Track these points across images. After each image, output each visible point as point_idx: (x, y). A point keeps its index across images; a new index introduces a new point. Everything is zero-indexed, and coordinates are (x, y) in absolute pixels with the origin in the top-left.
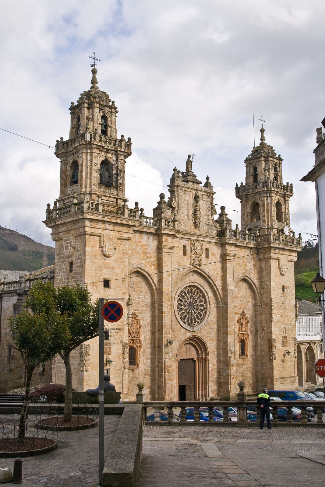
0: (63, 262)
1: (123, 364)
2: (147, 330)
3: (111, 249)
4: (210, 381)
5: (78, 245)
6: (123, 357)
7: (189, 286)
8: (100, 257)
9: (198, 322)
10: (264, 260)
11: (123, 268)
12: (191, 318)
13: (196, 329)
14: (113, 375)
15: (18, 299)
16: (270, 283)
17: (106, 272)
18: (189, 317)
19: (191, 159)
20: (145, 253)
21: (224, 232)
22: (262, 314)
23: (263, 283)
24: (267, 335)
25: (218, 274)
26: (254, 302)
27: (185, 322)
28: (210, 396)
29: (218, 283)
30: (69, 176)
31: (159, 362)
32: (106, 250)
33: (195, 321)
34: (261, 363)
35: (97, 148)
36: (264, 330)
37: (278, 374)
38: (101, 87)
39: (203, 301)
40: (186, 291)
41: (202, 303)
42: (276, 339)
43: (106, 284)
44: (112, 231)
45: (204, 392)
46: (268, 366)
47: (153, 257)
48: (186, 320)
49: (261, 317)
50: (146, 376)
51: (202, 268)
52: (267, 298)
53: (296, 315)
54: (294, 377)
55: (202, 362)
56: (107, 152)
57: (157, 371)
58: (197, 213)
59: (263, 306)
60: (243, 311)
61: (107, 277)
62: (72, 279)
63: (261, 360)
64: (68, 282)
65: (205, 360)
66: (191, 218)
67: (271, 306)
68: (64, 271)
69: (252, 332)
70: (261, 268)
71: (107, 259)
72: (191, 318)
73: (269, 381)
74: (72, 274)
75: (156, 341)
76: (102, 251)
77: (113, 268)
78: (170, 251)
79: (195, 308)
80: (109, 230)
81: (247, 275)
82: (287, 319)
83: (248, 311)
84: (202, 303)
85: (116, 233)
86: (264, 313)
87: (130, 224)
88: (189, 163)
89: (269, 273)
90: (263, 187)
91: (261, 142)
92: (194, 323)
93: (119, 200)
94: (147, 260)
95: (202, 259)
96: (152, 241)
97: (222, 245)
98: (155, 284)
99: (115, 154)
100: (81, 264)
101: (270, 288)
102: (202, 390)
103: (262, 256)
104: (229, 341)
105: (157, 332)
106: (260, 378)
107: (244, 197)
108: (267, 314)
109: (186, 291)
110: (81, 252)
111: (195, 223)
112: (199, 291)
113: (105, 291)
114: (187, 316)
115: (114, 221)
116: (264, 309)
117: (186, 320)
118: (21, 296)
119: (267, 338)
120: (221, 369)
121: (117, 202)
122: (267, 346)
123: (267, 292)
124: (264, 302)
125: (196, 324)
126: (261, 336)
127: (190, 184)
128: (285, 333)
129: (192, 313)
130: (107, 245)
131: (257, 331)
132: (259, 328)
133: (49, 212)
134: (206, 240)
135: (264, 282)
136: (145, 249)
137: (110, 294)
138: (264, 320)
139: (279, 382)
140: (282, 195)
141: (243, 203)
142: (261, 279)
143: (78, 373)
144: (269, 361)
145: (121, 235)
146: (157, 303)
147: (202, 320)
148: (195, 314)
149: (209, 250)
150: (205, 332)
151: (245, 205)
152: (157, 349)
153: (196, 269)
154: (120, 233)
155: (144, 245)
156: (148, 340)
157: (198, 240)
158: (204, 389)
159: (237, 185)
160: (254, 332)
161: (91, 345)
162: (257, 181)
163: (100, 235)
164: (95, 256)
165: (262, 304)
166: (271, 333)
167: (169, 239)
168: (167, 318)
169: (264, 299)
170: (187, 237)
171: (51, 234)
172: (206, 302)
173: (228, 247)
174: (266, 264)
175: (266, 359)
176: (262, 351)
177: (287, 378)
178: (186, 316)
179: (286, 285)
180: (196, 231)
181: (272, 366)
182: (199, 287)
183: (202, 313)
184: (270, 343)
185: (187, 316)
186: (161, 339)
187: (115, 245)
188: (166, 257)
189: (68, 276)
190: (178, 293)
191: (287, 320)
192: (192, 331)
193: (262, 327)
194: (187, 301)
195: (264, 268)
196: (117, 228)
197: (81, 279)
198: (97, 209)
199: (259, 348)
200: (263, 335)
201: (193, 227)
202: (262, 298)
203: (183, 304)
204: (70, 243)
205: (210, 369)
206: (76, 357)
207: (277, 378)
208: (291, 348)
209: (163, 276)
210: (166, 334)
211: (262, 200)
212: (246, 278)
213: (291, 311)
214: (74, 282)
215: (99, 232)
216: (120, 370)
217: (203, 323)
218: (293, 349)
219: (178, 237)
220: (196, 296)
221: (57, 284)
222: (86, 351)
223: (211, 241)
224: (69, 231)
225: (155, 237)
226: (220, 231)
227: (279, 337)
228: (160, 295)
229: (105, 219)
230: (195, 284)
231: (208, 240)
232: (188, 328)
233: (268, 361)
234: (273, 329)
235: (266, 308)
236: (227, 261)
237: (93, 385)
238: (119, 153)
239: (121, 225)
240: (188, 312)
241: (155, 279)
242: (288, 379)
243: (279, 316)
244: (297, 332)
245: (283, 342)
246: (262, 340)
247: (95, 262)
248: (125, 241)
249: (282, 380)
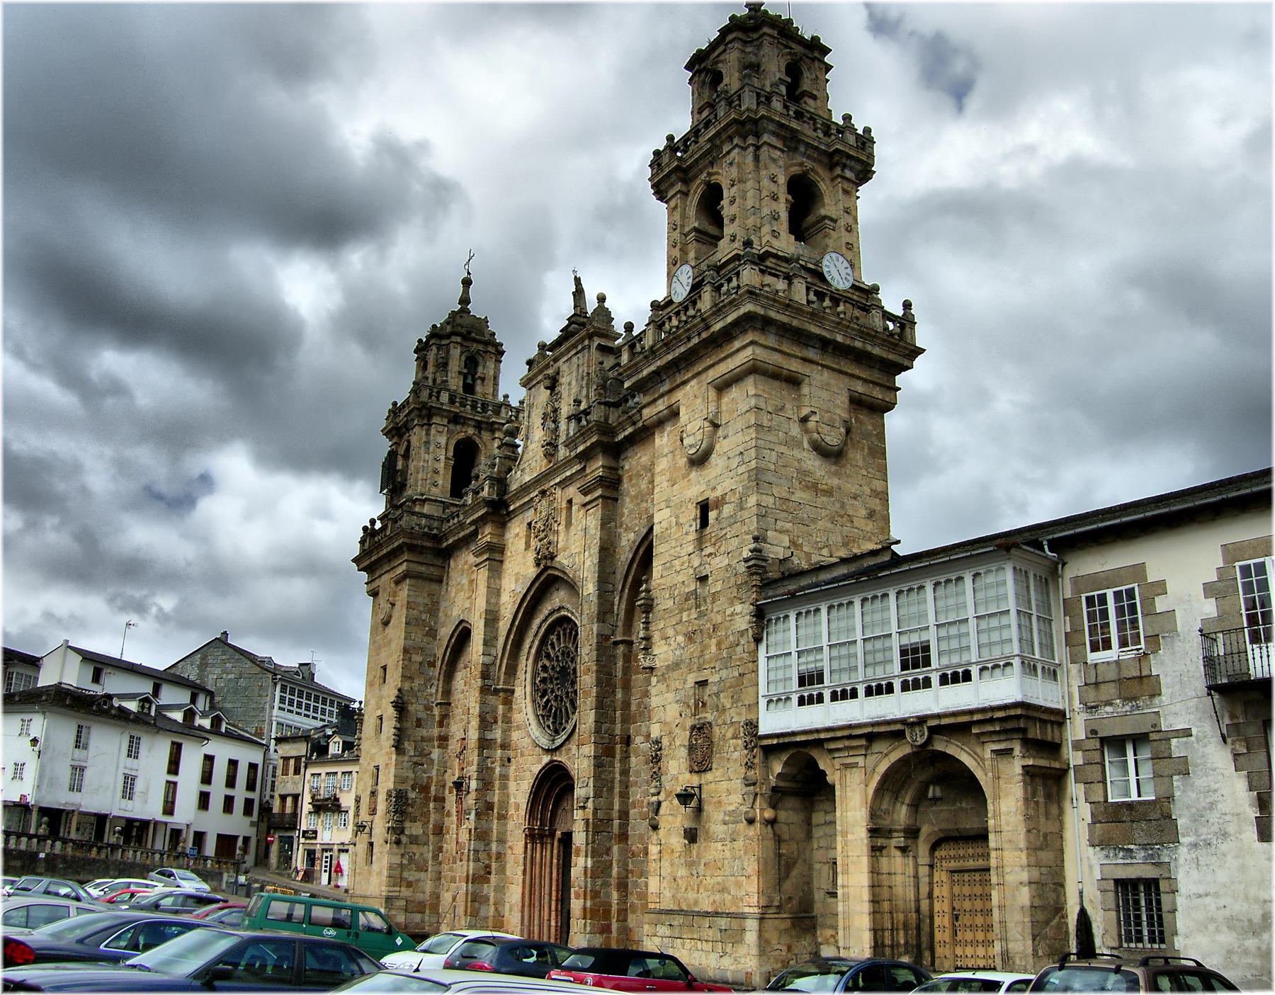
12: (561, 711)
18: (556, 711)
27: (548, 726)
37: (667, 894)
40: (554, 638)
42: (665, 742)
48: (551, 720)
54: (741, 917)
82: (714, 641)
85: (392, 575)
95: (551, 538)
109: (554, 640)
115: (381, 554)
117: (551, 720)
129: (562, 697)
134: (558, 480)
139: (663, 930)
149: (574, 501)
153: (550, 572)
170: (526, 499)
177: (706, 914)
178: (551, 709)
179: (718, 493)
190: (533, 651)
191: (713, 649)
207: (661, 912)
213: (732, 604)
216: (382, 845)
218: (738, 784)
223: (568, 473)
227: (678, 731)
230: (563, 613)
231: (563, 476)
234: (654, 701)
240: (556, 696)
242: (706, 922)
243: (680, 639)
245: (691, 748)
249: (678, 920)
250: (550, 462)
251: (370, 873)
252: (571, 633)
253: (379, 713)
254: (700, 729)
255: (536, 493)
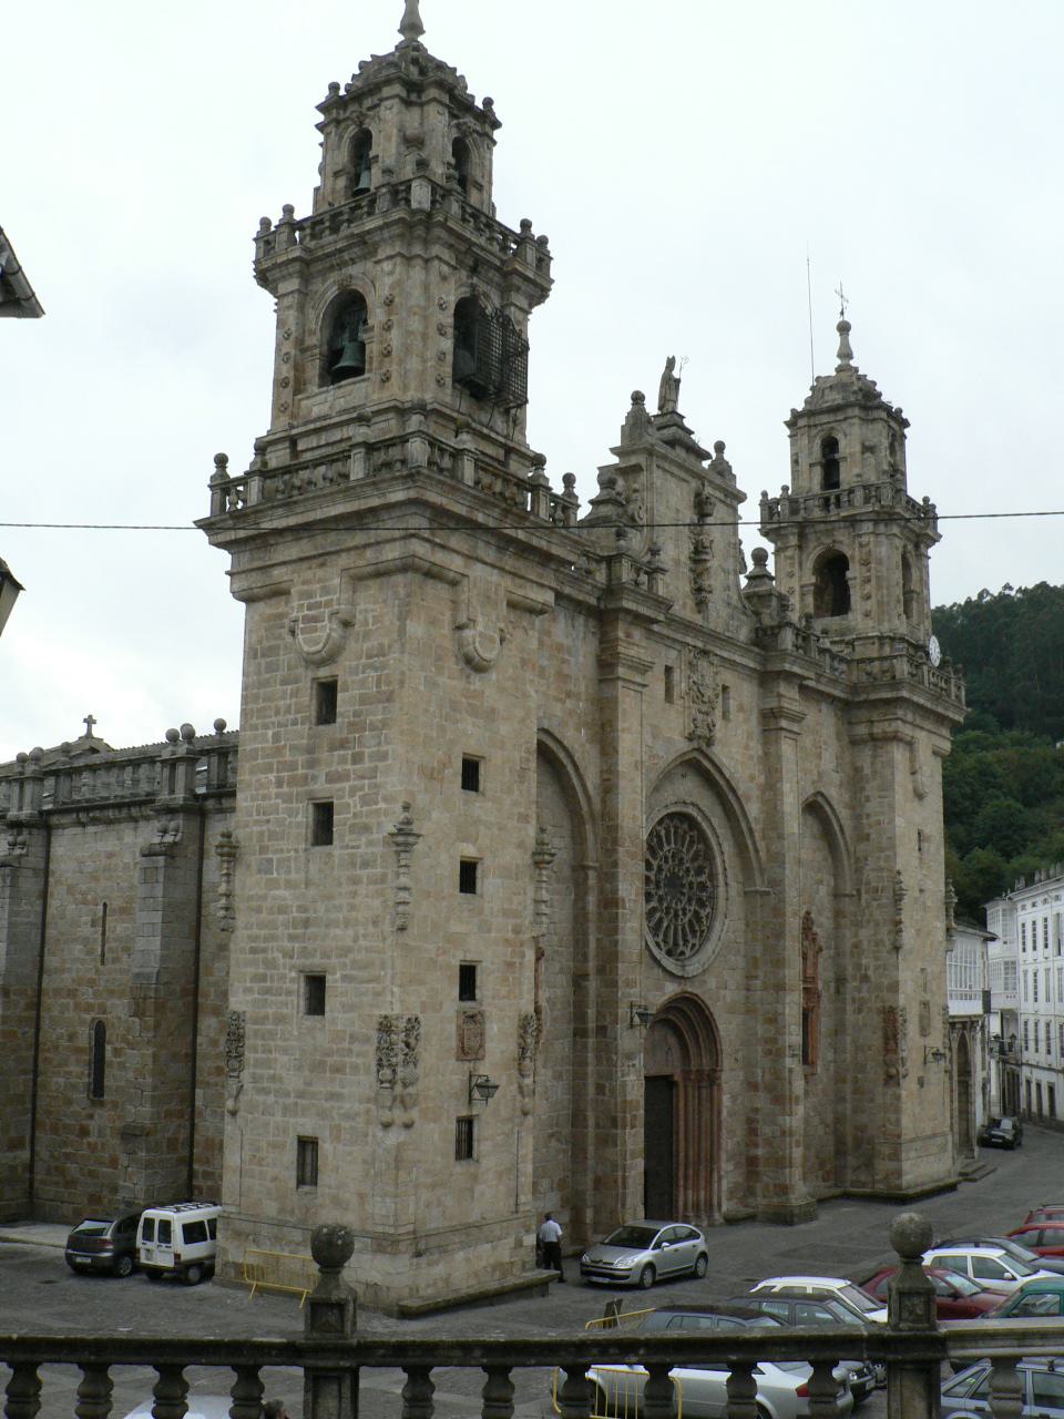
0: (285, 682)
1: (519, 1097)
2: (557, 967)
3: (491, 640)
4: (724, 1156)
5: (366, 611)
6: (520, 1070)
7: (671, 816)
8: (452, 665)
9: (694, 945)
10: (870, 744)
11: (523, 721)
12: (676, 929)
13: (693, 968)
14: (489, 1143)
15: (13, 845)
16: (892, 821)
17: (470, 727)
18: (668, 927)
19: (676, 374)
20: (563, 677)
21: (776, 635)
22: (858, 925)
23: (865, 821)
24: (877, 997)
25: (752, 778)
26: (832, 883)
27: (658, 944)
28: (724, 1208)
29: (753, 809)
30: (317, 351)
31: (600, 1089)
32: (478, 639)
33: (686, 941)
34: (855, 1092)
35: (451, 247)
36: (865, 979)
38: (436, 44)
39: (707, 871)
40: (663, 833)
41: (703, 878)
43: (471, 774)
44: (496, 571)
45: (702, 1193)
46: (879, 1100)
47: (583, 697)
49: (856, 936)
50: (554, 1143)
51: (719, 752)
52: (881, 869)
53: (948, 930)
54: (944, 1134)
55: (699, 1088)
56: (474, 270)
57: (591, 1122)
58: (704, 557)
59: (864, 896)
60: (808, 913)
61: (473, 748)
62: (332, 749)
63: (856, 1081)
64: (312, 764)
65: (711, 1079)
66: (686, 570)
67: (898, 898)
68: (291, 717)
69: (826, 983)
70: (857, 770)
71: (477, 682)
72: (676, 929)
73: (886, 1150)
74: (337, 730)
75: (591, 1013)
76: (461, 645)
77: (491, 715)
78: (638, 679)
79: (683, 894)
80: (485, 563)
81: (823, 790)
83: (820, 912)
84: (703, 878)
85: (507, 582)
86: (868, 921)
87: (555, 550)
88: (670, 385)
89: (887, 787)
90: (867, 500)
91: (838, 362)
92: (681, 948)
93: (513, 456)
94: (569, 704)
96: (581, 635)
97: (766, 678)
98: (589, 799)
99: (498, 286)
100: (384, 688)
101: (892, 839)
102: (696, 1189)
103: (862, 730)
104: (787, 1011)
105: (591, 977)
106: (849, 1140)
107: (793, 534)
108: (877, 924)
109: (663, 833)
110: (386, 642)
111: (699, 590)
112: (695, 833)
113: (466, 802)
114: (665, 925)
116: (868, 907)
117: (661, 937)
118: (25, 832)
119: (879, 1005)
120: (756, 1110)
121: (504, 464)
122: (880, 1034)
123: (882, 850)
124: (868, 883)
125: (688, 953)
126: (854, 1000)
127: (680, 453)
128: (925, 991)
130: (480, 619)
131: (840, 981)
132: (850, 971)
133: (223, 485)
134: (725, 654)
135: (868, 816)
136: (564, 661)
137: (484, 817)
138: (865, 943)
140: (913, 537)
141: (789, 553)
142: (856, 806)
143: (366, 1135)
144: (886, 1083)
145: (521, 592)
146: (594, 868)
147: (704, 938)
148: (684, 914)
149: (732, 693)
150: (712, 983)
151: (797, 561)
152: (591, 1041)
153: (696, 754)
154: (518, 581)
155: (560, 648)
156: (559, 1006)
157: (705, 653)
158: (702, 1183)
159: (765, 494)
160: (833, 985)
161: (421, 1018)
162: (836, 485)
163: (458, 577)
164: (439, 658)
165: (859, 891)
166: (894, 987)
167: (637, 634)
168: (629, 924)
169: (869, 874)
170: (679, 637)
171: (227, 573)
172: (712, 877)
173: (783, 688)
174: (874, 757)
175: (875, 1072)
176: (858, 1048)
177: (930, 1137)
178: (661, 920)
180: (697, 619)
181: (898, 1098)
182: (699, 819)
183: (703, 913)
184: (891, 1023)
185: (665, 925)
186: (608, 1004)
187: (502, 625)
188: (628, 700)
189: (310, 737)
192: (682, 977)
193: (858, 966)
194: (665, 867)
195: (867, 771)
196: (510, 562)
197: (384, 748)
198: (453, 473)
199: (849, 1039)
200: (864, 994)
201: (690, 603)
202: (859, 870)
203: (653, 878)
204: (328, 604)
205: (725, 1113)
206: (355, 1068)
208: (936, 1040)
209: (620, 768)
210: (627, 985)
211: (861, 546)
212: (820, 799)
214: (343, 760)
215: (456, 564)
216: (510, 1120)
217: (710, 947)
219: (653, 632)
220: (688, 851)
221: (252, 772)
222: (408, 1045)
224: (322, 557)
225: (592, 623)
226: (757, 629)
228: (604, 841)
229: (480, 518)
232: (669, 963)
233: (883, 1082)
235: (875, 903)
236: (784, 733)
237: (429, 1180)
238: (516, 280)
239: (525, 550)
240: (668, 908)
241: (592, 779)
244: (951, 987)
246: (860, 1011)
247: (435, 685)
248: (528, 615)
250: (699, 612)
251: (475, 1178)
252: (684, 838)
253: (470, 851)
254: (925, 1004)
255: (700, 645)
